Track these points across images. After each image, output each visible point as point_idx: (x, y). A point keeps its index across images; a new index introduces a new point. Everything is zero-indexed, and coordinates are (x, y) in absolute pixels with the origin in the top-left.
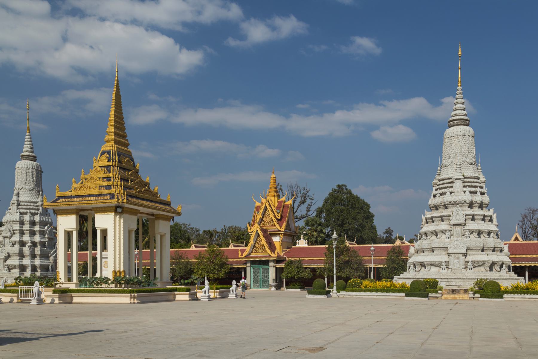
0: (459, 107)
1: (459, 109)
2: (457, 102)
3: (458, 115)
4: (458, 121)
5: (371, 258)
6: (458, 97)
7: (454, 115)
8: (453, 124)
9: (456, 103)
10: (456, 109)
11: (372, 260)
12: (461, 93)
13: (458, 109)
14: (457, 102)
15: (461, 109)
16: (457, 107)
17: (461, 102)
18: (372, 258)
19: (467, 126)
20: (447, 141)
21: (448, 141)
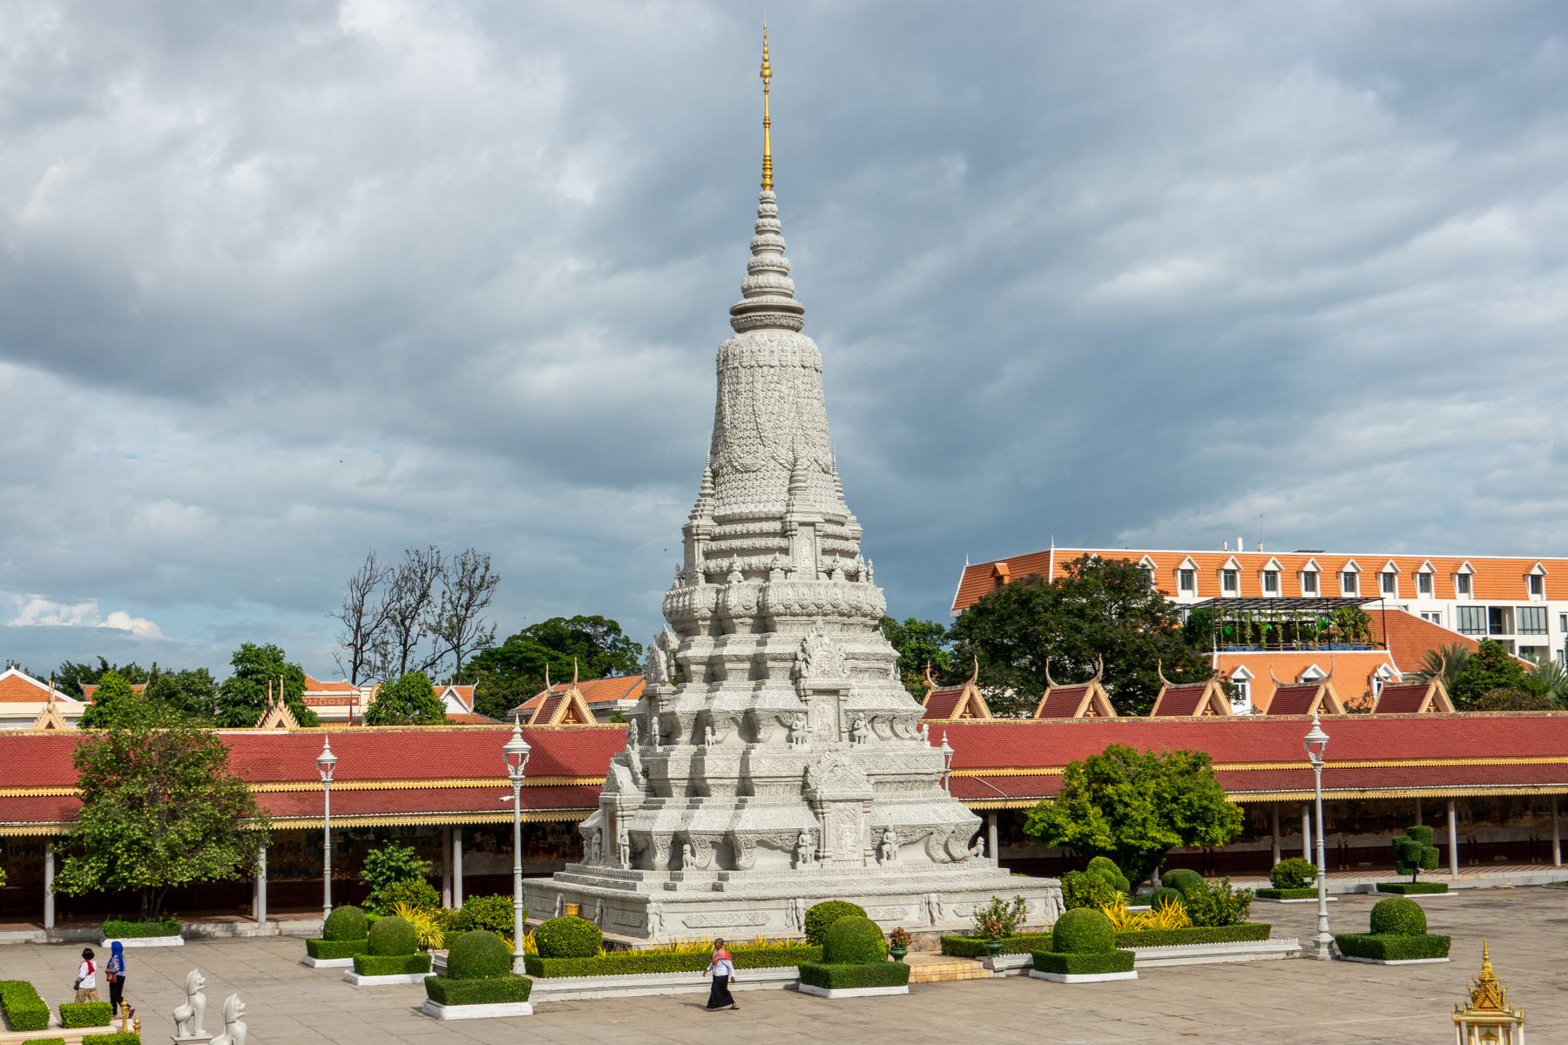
0: (775, 262)
1: (775, 268)
2: (768, 245)
3: (774, 290)
4: (781, 314)
5: (318, 786)
6: (770, 228)
7: (761, 287)
8: (761, 320)
9: (762, 245)
10: (766, 268)
11: (327, 793)
12: (775, 214)
13: (770, 268)
14: (768, 245)
15: (781, 269)
16: (768, 263)
17: (778, 246)
18: (327, 785)
19: (797, 331)
20: (743, 379)
21: (751, 379)
